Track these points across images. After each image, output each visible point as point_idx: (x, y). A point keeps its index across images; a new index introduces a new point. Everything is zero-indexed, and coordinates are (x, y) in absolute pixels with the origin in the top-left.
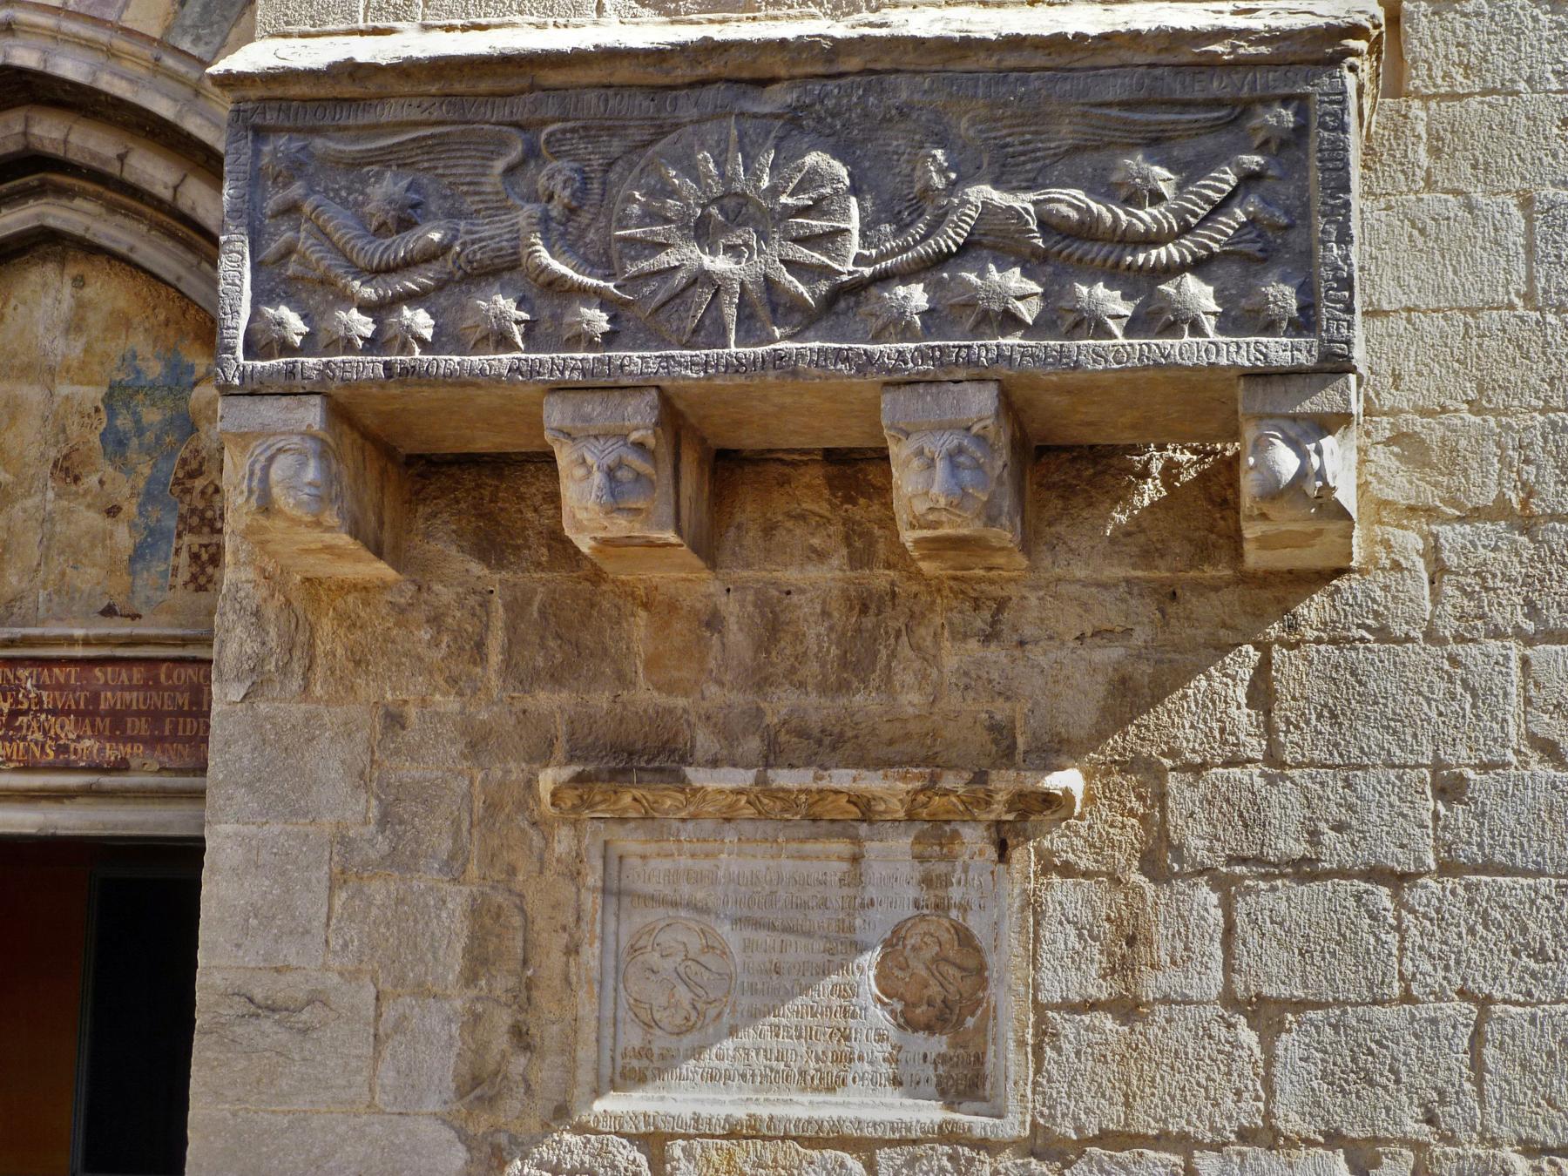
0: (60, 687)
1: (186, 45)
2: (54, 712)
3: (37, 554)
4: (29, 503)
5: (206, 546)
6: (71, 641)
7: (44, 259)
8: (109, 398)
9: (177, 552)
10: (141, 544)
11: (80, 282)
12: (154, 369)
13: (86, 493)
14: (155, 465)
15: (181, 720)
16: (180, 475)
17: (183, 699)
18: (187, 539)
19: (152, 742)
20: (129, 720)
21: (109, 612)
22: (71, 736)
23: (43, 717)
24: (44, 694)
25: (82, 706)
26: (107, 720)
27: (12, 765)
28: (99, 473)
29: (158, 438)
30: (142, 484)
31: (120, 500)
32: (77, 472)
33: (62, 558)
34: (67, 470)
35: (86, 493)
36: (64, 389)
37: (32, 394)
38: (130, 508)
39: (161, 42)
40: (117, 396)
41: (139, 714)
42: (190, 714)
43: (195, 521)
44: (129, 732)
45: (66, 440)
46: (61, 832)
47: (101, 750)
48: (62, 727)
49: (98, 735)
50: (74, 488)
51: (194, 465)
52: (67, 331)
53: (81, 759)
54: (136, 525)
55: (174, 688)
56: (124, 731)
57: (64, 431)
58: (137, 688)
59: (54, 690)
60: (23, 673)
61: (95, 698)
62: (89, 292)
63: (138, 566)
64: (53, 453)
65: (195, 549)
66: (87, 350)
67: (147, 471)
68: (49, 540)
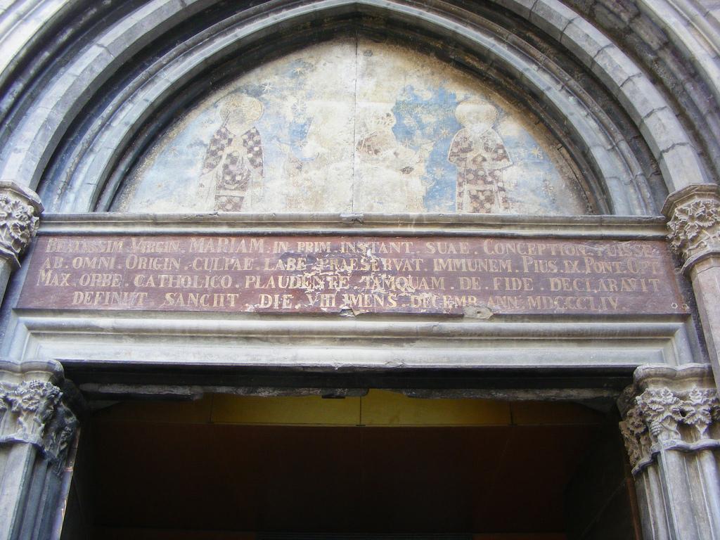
2: (393, 273)
3: (350, 193)
5: (482, 191)
6: (406, 221)
7: (343, 42)
9: (460, 194)
10: (431, 189)
13: (384, 160)
14: (435, 145)
15: (507, 279)
16: (455, 150)
17: (508, 265)
18: (466, 187)
19: (484, 294)
20: (461, 279)
22: (410, 290)
23: (384, 276)
24: (384, 261)
25: (418, 269)
26: (442, 279)
27: (357, 313)
28: (393, 149)
29: (435, 131)
30: (427, 155)
31: (411, 164)
32: (376, 148)
33: (369, 197)
34: (369, 147)
35: (384, 160)
36: (362, 104)
37: (341, 107)
38: (420, 169)
40: (399, 109)
41: (469, 274)
42: (513, 275)
43: (471, 177)
44: (462, 288)
45: (367, 131)
46: (410, 364)
47: (439, 301)
48: (402, 284)
49: (436, 290)
50: (375, 157)
51: (465, 145)
52: (363, 76)
53: (422, 307)
54: (426, 178)
55: (497, 257)
56: (457, 287)
57: (365, 125)
58: (465, 256)
59: (392, 257)
60: (363, 245)
61: (429, 263)
63: (431, 203)
64: (358, 137)
65: (474, 193)
66: (378, 85)
67: (430, 148)
68: (359, 186)
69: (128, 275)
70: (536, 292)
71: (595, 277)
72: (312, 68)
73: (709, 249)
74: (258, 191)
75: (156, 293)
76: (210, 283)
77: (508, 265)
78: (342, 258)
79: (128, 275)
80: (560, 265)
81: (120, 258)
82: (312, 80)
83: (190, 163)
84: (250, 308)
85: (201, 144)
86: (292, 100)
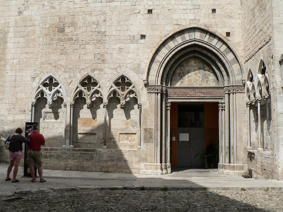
0: (199, 91)
1: (209, 43)
2: (199, 92)
4: (193, 77)
8: (198, 68)
11: (195, 60)
12: (202, 66)
17: (209, 91)
21: (200, 85)
36: (195, 68)
38: (201, 77)
39: (207, 42)
43: (206, 78)
49: (202, 94)
62: (196, 60)
66: (196, 65)
69: (175, 93)
70: (211, 94)
71: (217, 93)
72: (189, 62)
73: (226, 93)
74: (185, 80)
75: (178, 95)
76: (183, 94)
77: (209, 91)
78: (194, 91)
79: (175, 93)
80: (214, 91)
81: (174, 91)
82: (190, 64)
83: (177, 76)
84: (187, 96)
85: (178, 74)
86: (187, 67)
